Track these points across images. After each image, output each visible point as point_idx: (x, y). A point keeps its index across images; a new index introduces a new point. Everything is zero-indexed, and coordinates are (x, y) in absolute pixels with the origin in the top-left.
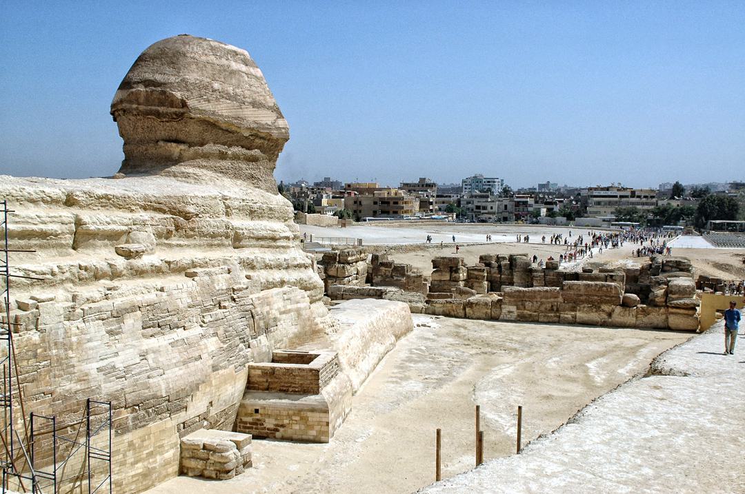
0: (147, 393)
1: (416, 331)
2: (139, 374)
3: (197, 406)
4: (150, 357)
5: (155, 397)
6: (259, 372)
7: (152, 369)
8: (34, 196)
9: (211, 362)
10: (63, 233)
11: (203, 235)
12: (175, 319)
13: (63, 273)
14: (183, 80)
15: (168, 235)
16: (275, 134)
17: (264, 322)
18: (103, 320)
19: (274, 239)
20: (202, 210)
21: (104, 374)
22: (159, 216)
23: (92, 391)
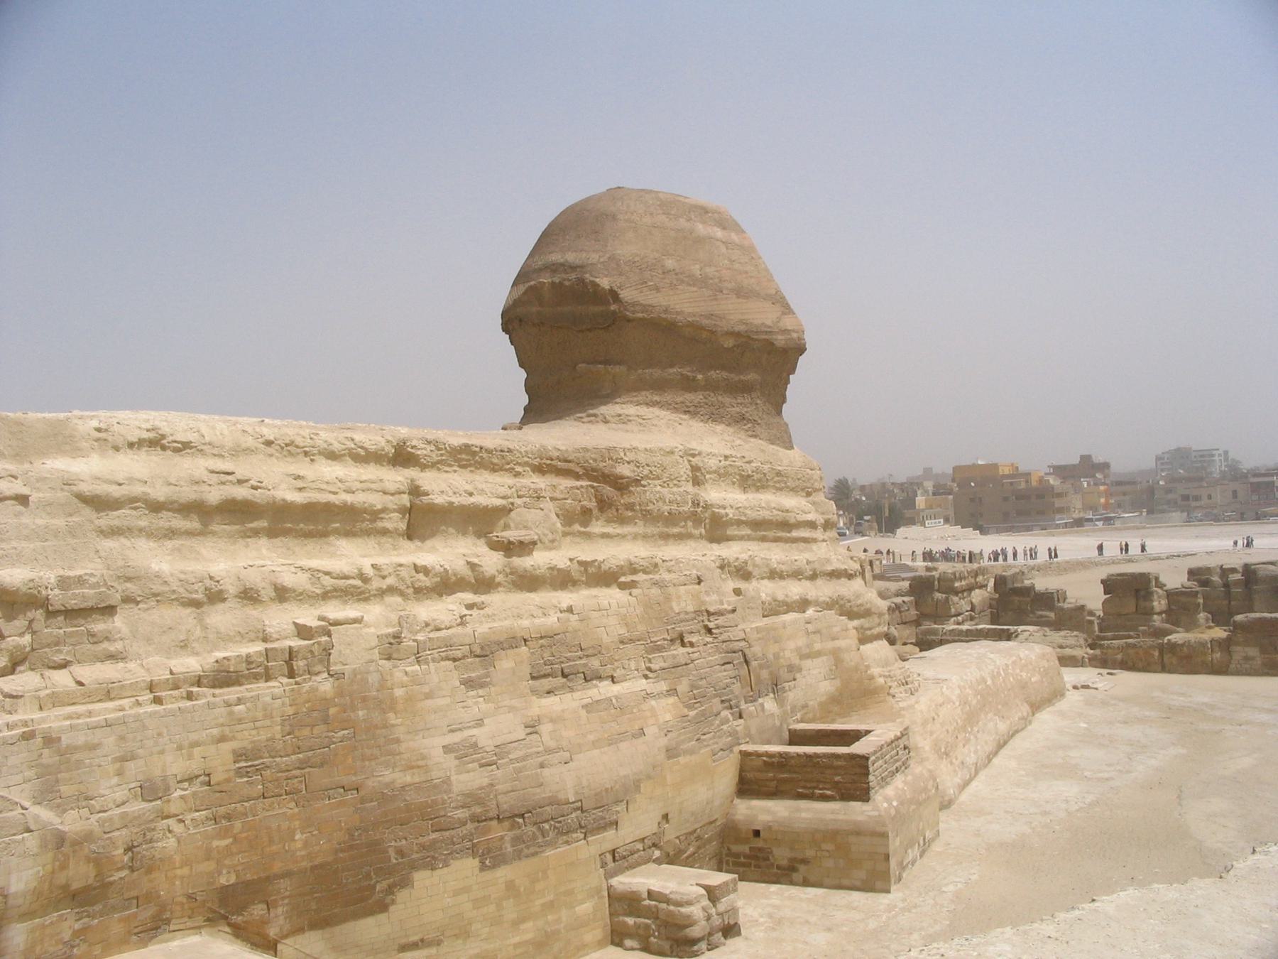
0: (541, 794)
1: (1073, 697)
2: (524, 759)
3: (638, 822)
4: (545, 728)
5: (553, 801)
6: (758, 762)
7: (549, 751)
8: (337, 447)
9: (663, 741)
10: (384, 510)
11: (648, 516)
12: (595, 663)
13: (384, 577)
14: (611, 258)
15: (585, 515)
16: (780, 340)
17: (771, 673)
18: (455, 660)
19: (786, 525)
20: (646, 472)
21: (457, 758)
22: (566, 483)
23: (435, 786)
